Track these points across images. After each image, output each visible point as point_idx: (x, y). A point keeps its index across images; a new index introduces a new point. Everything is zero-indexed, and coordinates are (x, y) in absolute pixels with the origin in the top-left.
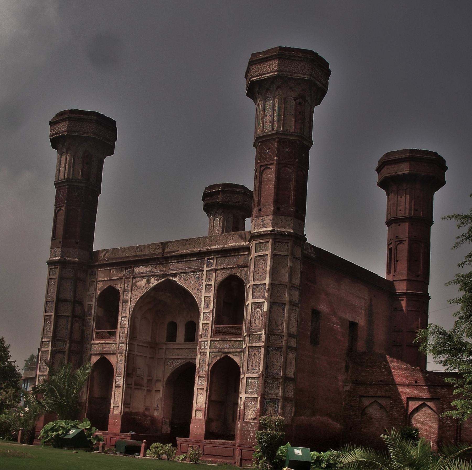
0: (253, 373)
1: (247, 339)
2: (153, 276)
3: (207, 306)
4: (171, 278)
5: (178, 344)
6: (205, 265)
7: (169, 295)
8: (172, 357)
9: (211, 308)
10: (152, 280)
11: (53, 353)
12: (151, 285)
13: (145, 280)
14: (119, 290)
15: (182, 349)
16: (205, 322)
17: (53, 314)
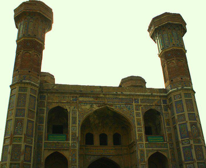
2: (96, 104)
3: (139, 124)
4: (109, 106)
5: (96, 146)
6: (134, 102)
7: (95, 116)
8: (90, 154)
9: (142, 125)
10: (95, 106)
11: (26, 146)
12: (94, 109)
13: (88, 107)
14: (67, 110)
15: (98, 149)
16: (140, 133)
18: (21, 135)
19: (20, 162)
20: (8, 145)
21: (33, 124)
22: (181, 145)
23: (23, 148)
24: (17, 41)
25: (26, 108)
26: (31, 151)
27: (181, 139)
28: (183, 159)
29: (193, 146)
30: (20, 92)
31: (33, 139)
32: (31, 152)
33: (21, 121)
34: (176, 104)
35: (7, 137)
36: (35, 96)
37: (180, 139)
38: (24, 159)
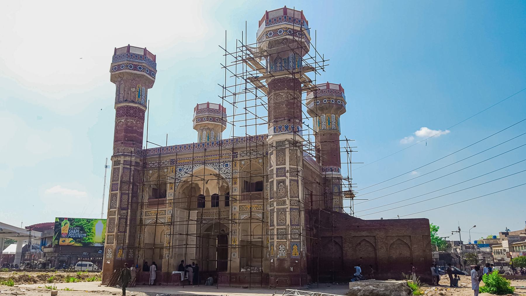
1: (275, 204)
11: (120, 219)
17: (118, 192)
18: (116, 208)
21: (128, 196)
23: (116, 221)
25: (119, 182)
29: (275, 210)
31: (129, 211)
33: (116, 195)
38: (118, 230)
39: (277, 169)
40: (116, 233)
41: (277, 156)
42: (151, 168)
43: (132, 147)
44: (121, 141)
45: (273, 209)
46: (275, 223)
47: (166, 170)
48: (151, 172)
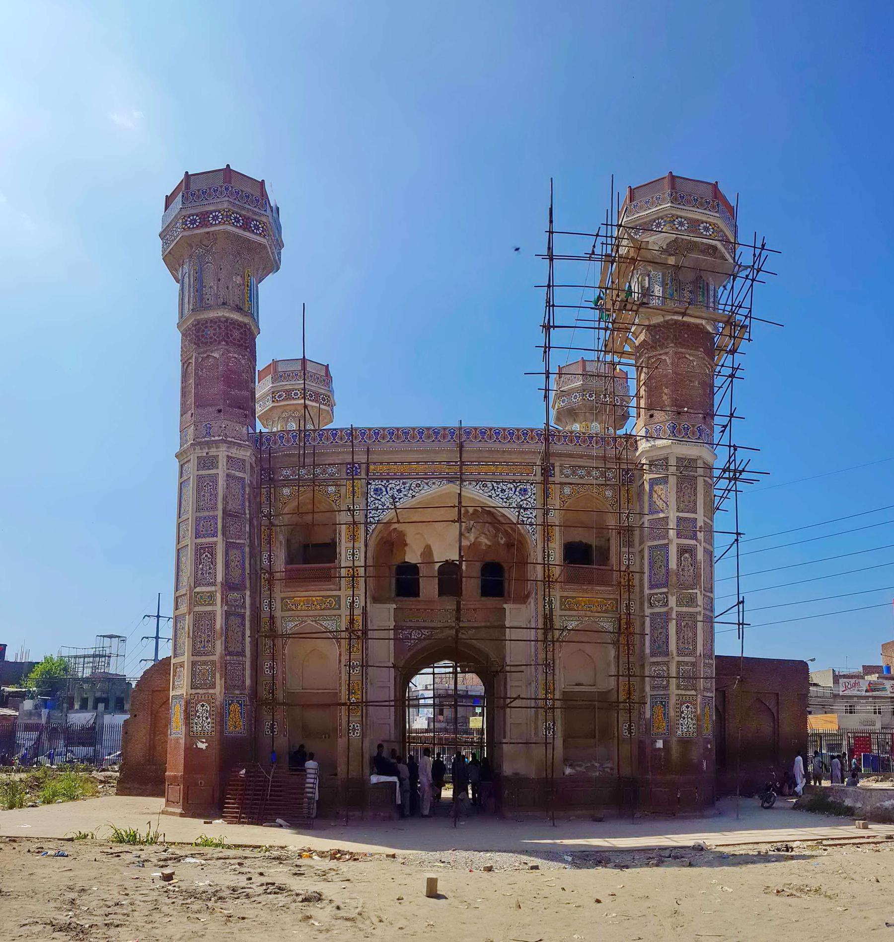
0: (686, 655)
19: (216, 658)
20: (184, 615)
22: (646, 604)
24: (179, 326)
26: (244, 626)
27: (650, 589)
28: (648, 651)
30: (201, 472)
32: (244, 629)
34: (651, 486)
35: (182, 591)
36: (241, 475)
37: (647, 591)
38: (226, 648)
39: (679, 519)
40: (221, 658)
41: (679, 490)
42: (287, 482)
43: (243, 424)
44: (217, 405)
45: (667, 614)
46: (673, 647)
47: (332, 489)
48: (286, 491)
